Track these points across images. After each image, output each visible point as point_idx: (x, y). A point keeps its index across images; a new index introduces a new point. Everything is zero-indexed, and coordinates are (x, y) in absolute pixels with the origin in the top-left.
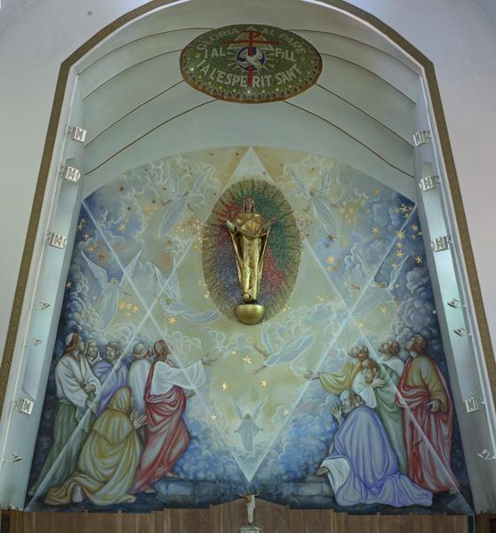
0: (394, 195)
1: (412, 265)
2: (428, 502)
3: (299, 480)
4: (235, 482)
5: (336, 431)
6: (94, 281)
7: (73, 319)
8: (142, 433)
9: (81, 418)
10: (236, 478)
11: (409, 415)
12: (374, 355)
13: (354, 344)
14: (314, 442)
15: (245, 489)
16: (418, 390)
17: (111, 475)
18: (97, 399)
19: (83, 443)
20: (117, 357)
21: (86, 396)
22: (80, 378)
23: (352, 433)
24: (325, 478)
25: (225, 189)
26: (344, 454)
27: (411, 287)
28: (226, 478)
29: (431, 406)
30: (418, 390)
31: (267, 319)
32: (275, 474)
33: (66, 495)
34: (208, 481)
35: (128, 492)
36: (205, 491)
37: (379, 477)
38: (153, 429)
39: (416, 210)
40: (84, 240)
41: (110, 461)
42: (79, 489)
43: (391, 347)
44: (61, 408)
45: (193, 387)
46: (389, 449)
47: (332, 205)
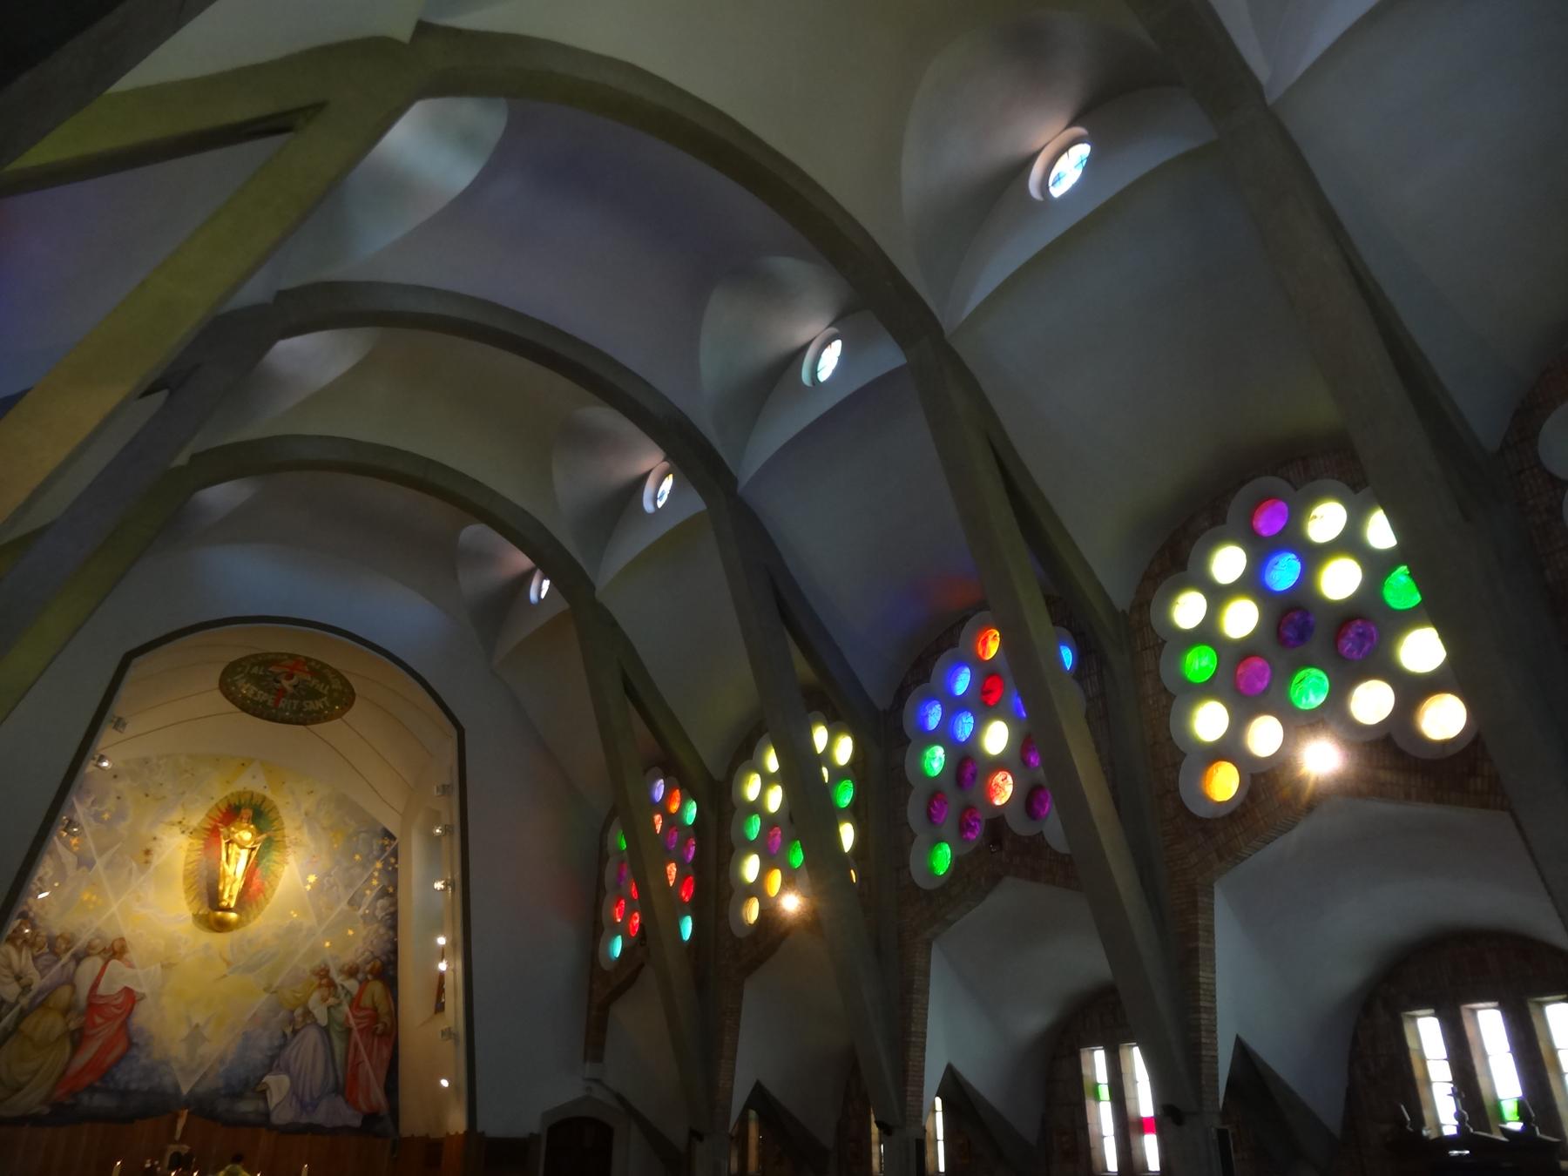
1: (383, 893)
2: (357, 1123)
3: (235, 1095)
5: (282, 1047)
11: (356, 1035)
12: (333, 974)
13: (317, 962)
18: (31, 994)
20: (67, 950)
24: (263, 1095)
26: (287, 1071)
27: (380, 914)
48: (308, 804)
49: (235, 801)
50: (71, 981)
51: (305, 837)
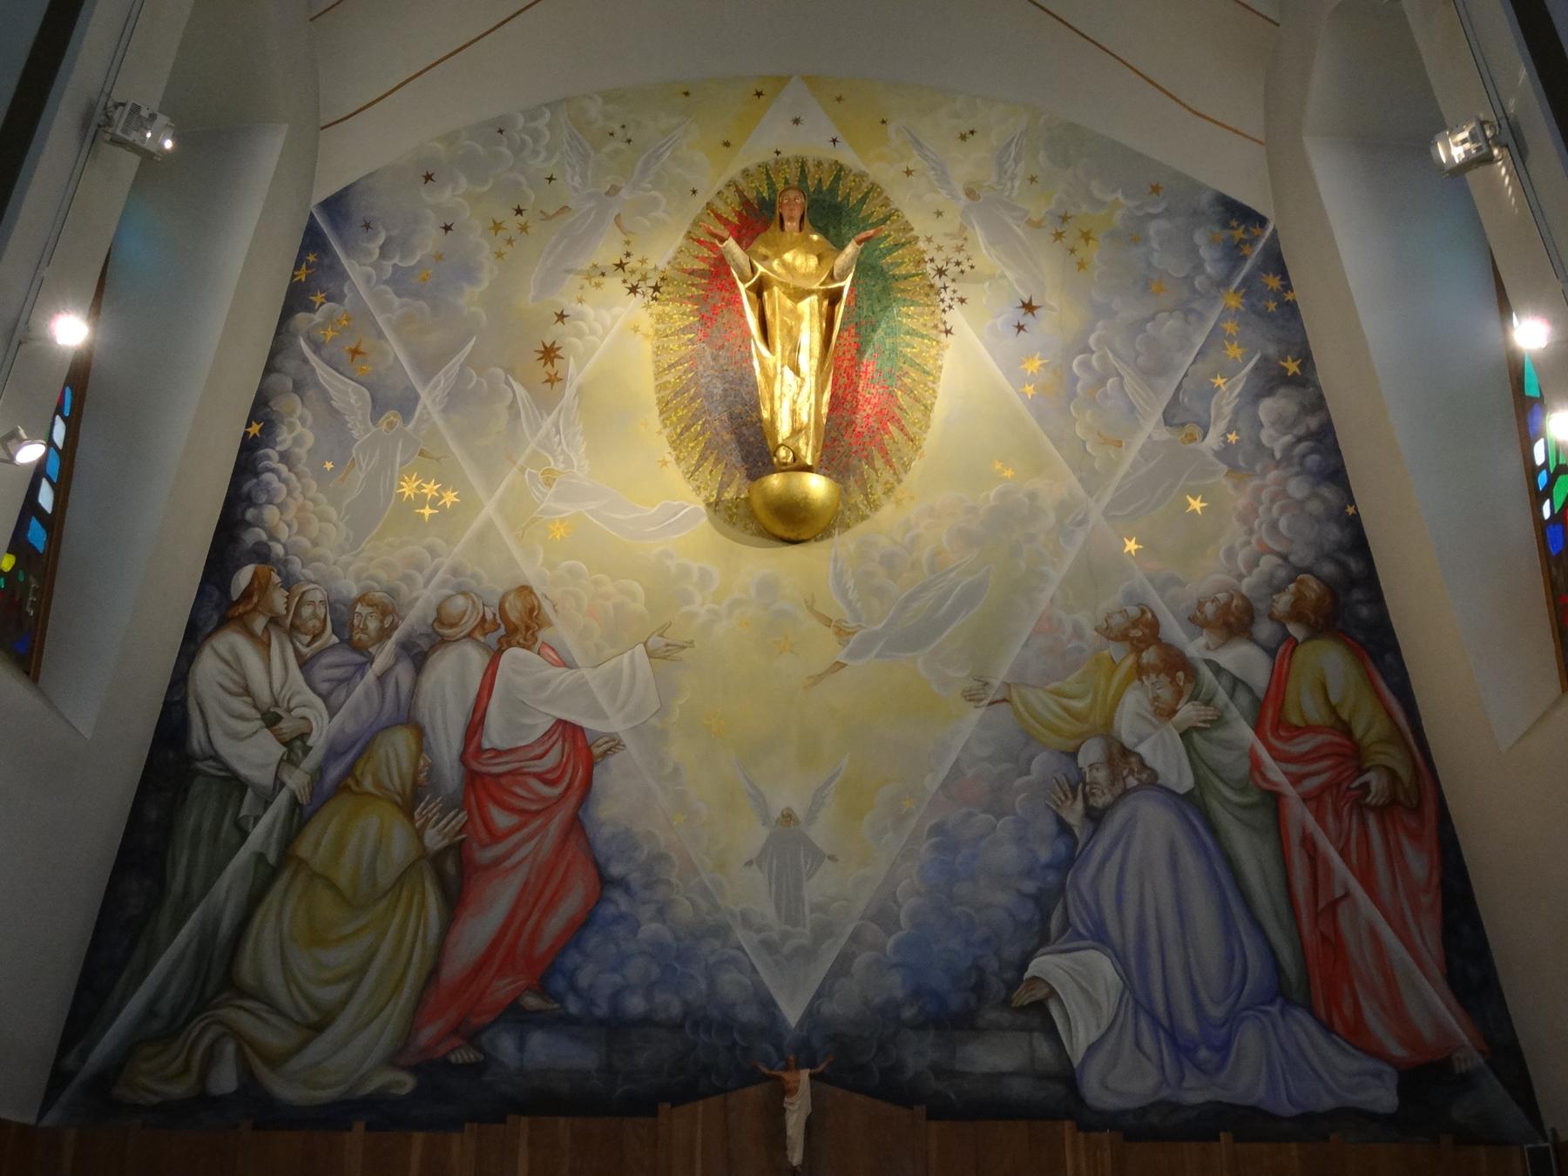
0: (1206, 198)
1: (1270, 380)
2: (1383, 1097)
3: (954, 1022)
6: (333, 417)
7: (259, 522)
8: (450, 866)
9: (257, 819)
10: (749, 1014)
11: (1299, 814)
12: (1174, 631)
13: (1112, 602)
14: (1002, 898)
16: (1320, 739)
17: (340, 991)
19: (255, 899)
20: (384, 634)
21: (279, 751)
22: (265, 697)
23: (1122, 870)
24: (1038, 1015)
25: (725, 179)
26: (1100, 938)
27: (1275, 441)
29: (1366, 787)
30: (1320, 739)
31: (848, 527)
33: (186, 1068)
35: (393, 1061)
37: (1216, 1012)
38: (486, 855)
39: (1275, 231)
40: (310, 308)
41: (341, 957)
42: (230, 1048)
43: (1225, 609)
44: (198, 787)
45: (615, 724)
46: (1243, 925)
47: (1030, 223)
48: (967, 164)
49: (756, 189)
50: (408, 718)
51: (984, 255)
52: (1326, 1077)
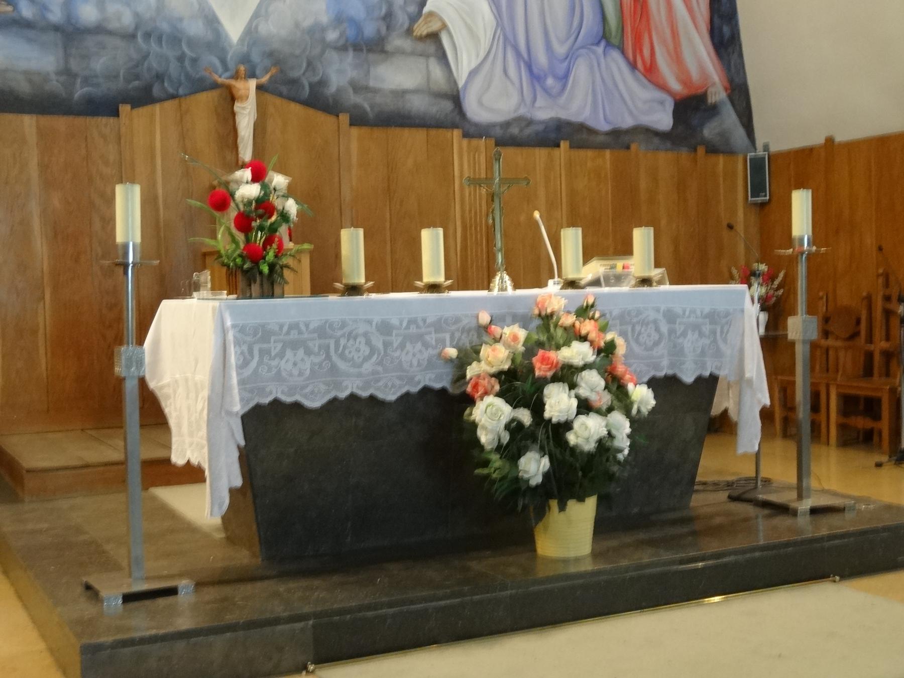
4: (191, 42)
10: (195, 28)
15: (223, 62)
28: (165, 27)
32: (307, 23)
34: (110, 33)
36: (105, 64)
37: (561, 50)
52: (629, 102)
